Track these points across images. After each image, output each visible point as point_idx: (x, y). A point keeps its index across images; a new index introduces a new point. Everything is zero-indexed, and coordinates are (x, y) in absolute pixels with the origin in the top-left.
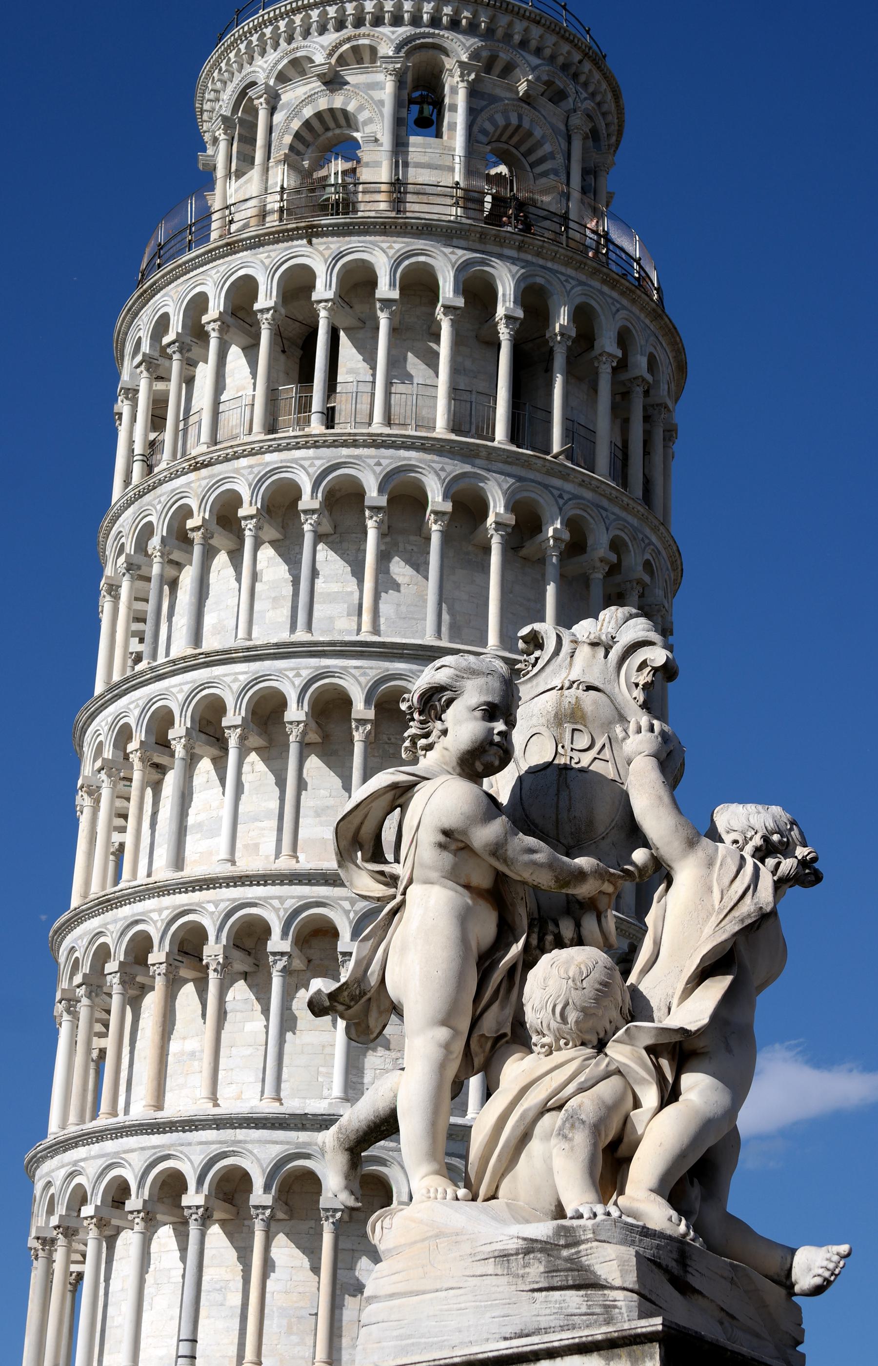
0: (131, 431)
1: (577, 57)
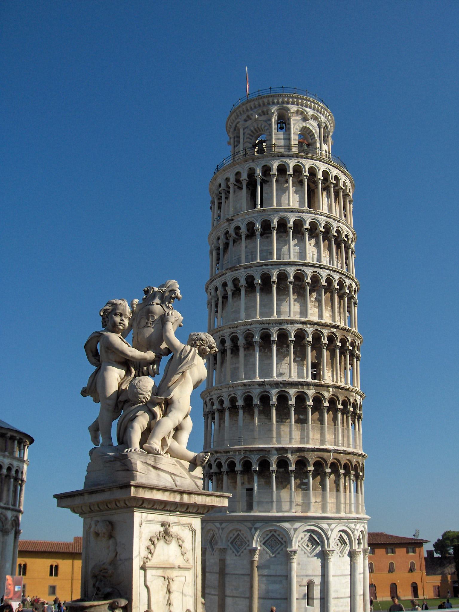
1: (320, 108)
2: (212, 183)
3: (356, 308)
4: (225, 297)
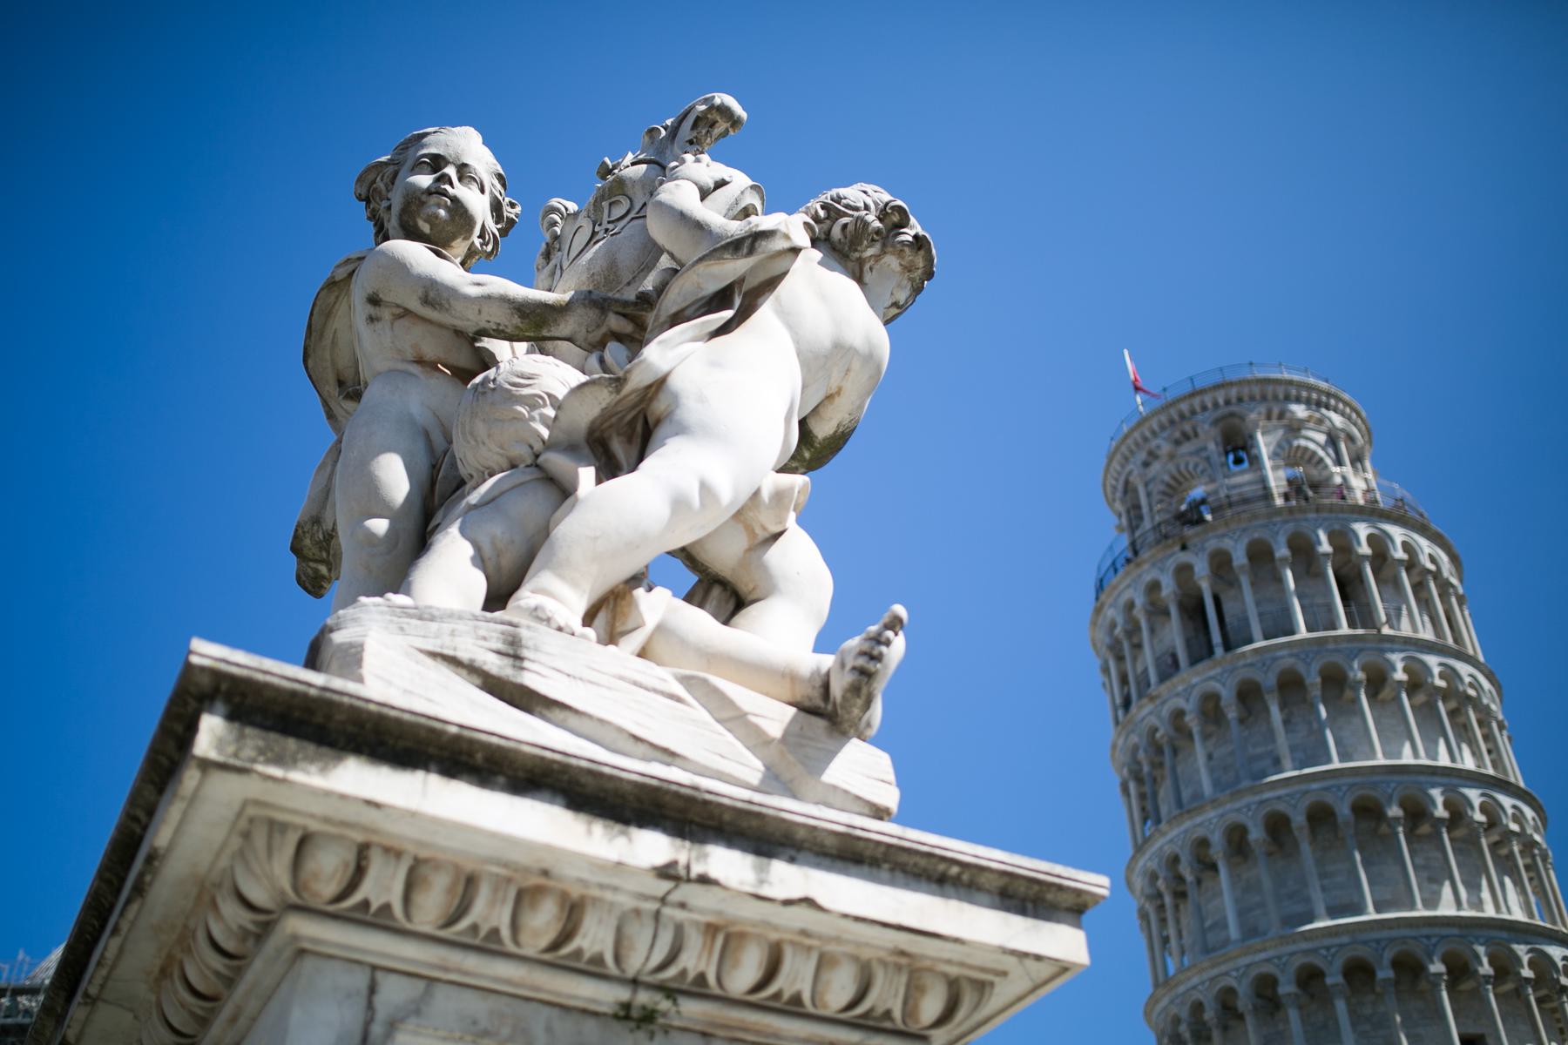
1: (1324, 399)
2: (1094, 623)
3: (1552, 873)
4: (1180, 895)
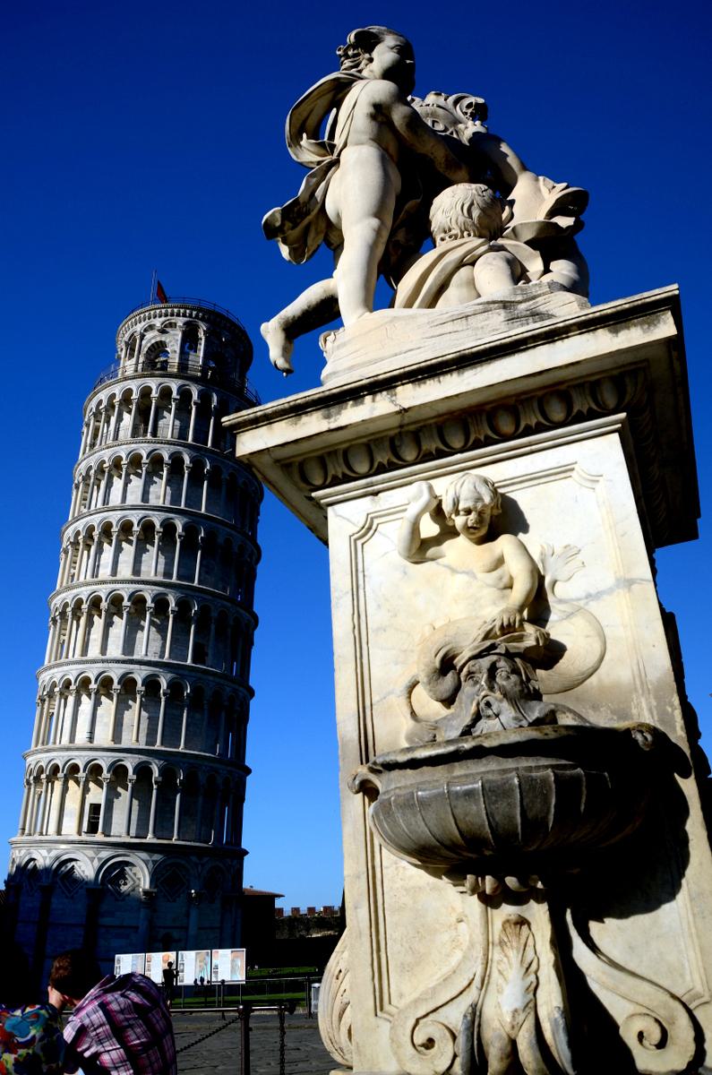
0: (86, 439)
